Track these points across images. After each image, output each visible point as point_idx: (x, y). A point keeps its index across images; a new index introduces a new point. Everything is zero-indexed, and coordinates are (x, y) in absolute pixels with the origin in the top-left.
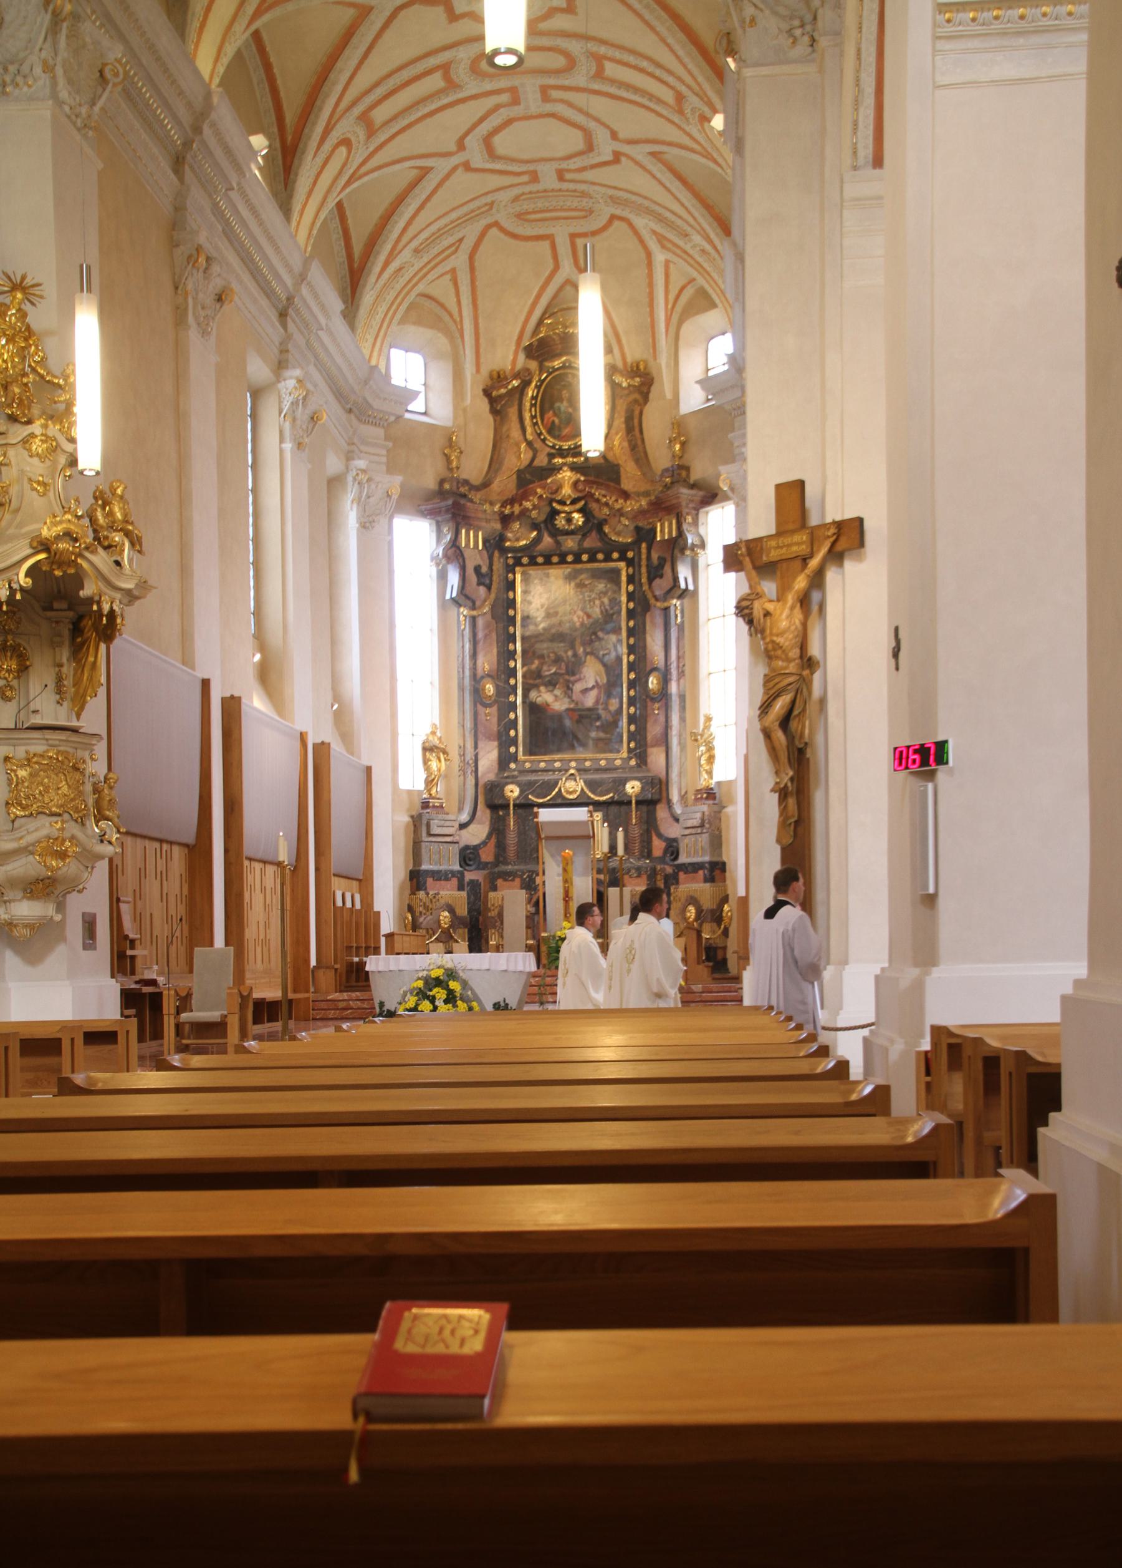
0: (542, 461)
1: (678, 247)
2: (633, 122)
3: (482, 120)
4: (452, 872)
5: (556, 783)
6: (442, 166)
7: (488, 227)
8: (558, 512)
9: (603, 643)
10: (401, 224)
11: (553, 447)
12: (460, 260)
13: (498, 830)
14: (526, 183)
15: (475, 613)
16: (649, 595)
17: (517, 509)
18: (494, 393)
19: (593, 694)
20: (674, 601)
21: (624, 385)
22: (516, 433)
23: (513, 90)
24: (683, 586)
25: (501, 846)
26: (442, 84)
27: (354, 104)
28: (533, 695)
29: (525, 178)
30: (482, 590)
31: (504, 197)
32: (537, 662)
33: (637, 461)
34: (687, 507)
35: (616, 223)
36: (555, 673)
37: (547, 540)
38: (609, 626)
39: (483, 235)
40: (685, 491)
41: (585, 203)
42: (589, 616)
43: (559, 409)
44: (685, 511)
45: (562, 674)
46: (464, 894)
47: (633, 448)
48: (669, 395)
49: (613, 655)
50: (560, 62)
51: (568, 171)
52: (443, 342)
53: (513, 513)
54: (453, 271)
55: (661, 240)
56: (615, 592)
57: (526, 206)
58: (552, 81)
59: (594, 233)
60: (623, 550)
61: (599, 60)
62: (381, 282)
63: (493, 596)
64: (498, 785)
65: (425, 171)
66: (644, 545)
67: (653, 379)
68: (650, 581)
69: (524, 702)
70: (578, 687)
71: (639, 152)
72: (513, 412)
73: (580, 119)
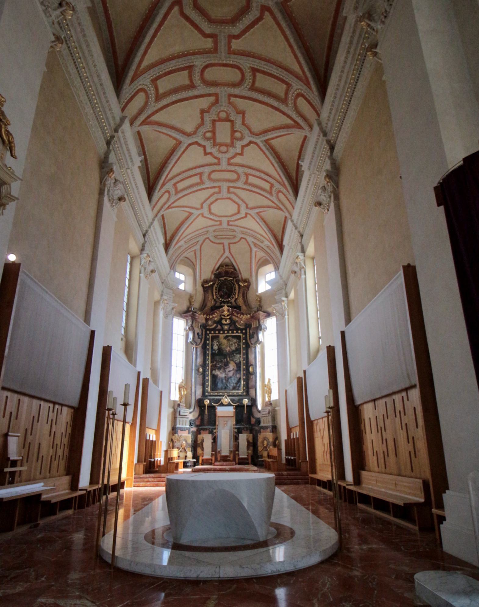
0: (218, 304)
2: (254, 200)
3: (209, 198)
5: (221, 399)
10: (182, 231)
12: (197, 247)
13: (202, 413)
14: (218, 225)
16: (250, 343)
17: (211, 317)
19: (232, 372)
22: (210, 297)
23: (219, 187)
24: (260, 340)
25: (202, 420)
26: (199, 181)
28: (214, 372)
29: (218, 223)
30: (199, 340)
33: (246, 306)
37: (219, 327)
38: (237, 352)
39: (204, 241)
40: (261, 312)
41: (234, 233)
46: (190, 435)
47: (245, 302)
48: (255, 288)
49: (238, 361)
50: (235, 176)
51: (231, 221)
52: (191, 271)
54: (195, 250)
55: (255, 245)
57: (217, 233)
59: (235, 243)
60: (241, 330)
61: (247, 175)
62: (174, 249)
65: (191, 214)
66: (248, 329)
68: (250, 339)
70: (227, 370)
73: (237, 200)
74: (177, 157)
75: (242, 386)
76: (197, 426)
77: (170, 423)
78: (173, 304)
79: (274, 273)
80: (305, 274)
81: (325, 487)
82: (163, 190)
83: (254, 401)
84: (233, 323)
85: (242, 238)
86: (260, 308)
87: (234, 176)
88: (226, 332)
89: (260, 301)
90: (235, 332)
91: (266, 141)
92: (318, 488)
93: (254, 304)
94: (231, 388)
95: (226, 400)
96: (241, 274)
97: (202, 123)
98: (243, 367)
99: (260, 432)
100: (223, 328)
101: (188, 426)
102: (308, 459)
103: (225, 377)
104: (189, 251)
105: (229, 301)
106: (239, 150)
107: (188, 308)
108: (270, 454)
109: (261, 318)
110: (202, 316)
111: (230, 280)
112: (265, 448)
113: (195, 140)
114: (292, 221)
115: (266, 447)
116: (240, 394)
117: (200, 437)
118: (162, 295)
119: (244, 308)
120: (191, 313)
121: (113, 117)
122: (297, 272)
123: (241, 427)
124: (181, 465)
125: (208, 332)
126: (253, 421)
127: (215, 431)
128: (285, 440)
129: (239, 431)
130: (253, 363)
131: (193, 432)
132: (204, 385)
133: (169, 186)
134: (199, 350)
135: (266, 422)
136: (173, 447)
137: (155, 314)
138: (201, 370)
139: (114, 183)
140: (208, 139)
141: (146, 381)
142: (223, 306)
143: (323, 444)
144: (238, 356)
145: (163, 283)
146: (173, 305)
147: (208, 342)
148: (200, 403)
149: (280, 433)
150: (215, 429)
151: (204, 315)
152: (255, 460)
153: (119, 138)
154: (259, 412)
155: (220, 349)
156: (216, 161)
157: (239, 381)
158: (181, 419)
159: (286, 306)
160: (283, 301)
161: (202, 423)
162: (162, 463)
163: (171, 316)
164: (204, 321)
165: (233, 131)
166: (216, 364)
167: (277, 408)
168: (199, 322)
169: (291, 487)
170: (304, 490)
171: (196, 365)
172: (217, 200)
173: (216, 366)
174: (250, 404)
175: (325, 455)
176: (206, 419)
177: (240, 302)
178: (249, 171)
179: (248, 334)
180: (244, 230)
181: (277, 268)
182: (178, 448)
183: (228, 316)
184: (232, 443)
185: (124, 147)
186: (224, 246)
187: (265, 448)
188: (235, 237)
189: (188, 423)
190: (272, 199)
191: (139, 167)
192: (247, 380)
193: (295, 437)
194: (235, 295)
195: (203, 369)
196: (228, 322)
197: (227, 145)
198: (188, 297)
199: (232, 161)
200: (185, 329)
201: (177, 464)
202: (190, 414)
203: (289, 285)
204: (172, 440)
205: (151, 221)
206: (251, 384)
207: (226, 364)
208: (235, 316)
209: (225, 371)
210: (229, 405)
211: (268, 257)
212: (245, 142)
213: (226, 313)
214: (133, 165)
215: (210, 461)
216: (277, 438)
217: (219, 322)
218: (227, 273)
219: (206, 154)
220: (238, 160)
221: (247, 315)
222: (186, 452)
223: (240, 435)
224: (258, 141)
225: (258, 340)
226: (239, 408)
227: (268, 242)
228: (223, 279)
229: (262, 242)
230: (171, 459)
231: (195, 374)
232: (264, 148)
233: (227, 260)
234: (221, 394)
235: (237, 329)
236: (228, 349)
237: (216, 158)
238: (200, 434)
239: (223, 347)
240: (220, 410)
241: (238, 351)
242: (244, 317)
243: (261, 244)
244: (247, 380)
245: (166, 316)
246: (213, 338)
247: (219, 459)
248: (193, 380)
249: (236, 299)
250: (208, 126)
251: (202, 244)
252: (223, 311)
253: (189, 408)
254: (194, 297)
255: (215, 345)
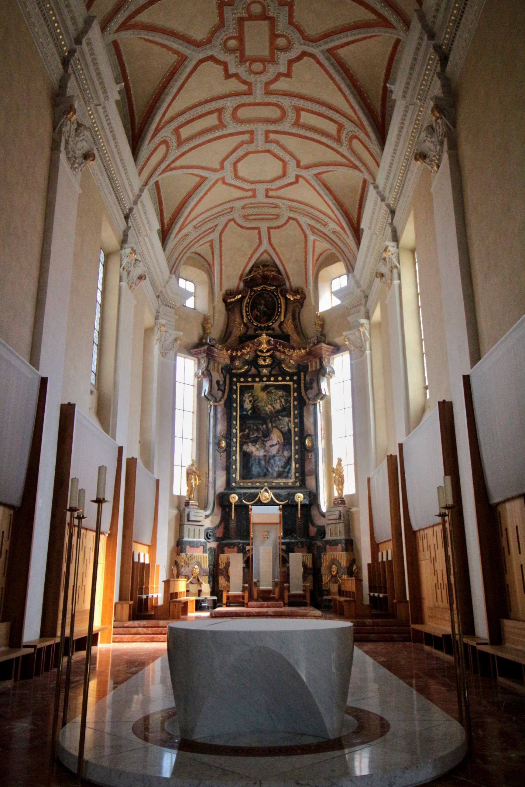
0: (251, 332)
1: (321, 232)
2: (310, 152)
4: (200, 542)
5: (257, 494)
6: (212, 177)
7: (230, 221)
8: (259, 356)
9: (281, 421)
10: (189, 209)
11: (257, 326)
12: (215, 236)
13: (225, 519)
14: (250, 197)
15: (216, 404)
16: (305, 397)
17: (239, 353)
18: (229, 301)
19: (277, 446)
20: (319, 401)
21: (292, 299)
22: (238, 320)
23: (251, 133)
24: (324, 393)
25: (227, 529)
27: (172, 119)
28: (245, 447)
29: (250, 193)
31: (238, 204)
32: (247, 430)
33: (298, 334)
34: (325, 354)
35: (291, 221)
36: (257, 436)
37: (253, 371)
38: (284, 413)
39: (226, 226)
41: (277, 211)
42: (274, 408)
43: (260, 309)
44: (324, 356)
45: (260, 437)
46: (206, 555)
47: (296, 327)
48: (313, 304)
49: (287, 428)
51: (272, 190)
52: (204, 276)
53: (237, 355)
54: (211, 241)
56: (287, 396)
57: (249, 211)
58: (272, 127)
59: (278, 227)
60: (291, 375)
63: (226, 396)
64: (225, 495)
65: (204, 179)
66: (302, 373)
67: (305, 295)
68: (306, 390)
69: (240, 451)
70: (268, 444)
71: (309, 174)
72: (237, 310)
74: (179, 83)
75: (293, 471)
76: (217, 539)
77: (173, 534)
78: (175, 332)
79: (345, 277)
80: (399, 279)
81: (438, 647)
82: (157, 140)
83: (313, 497)
84: (276, 363)
85: (290, 218)
86: (322, 337)
87: (276, 113)
88: (265, 379)
89: (322, 326)
90: (280, 378)
91: (329, 51)
92: (427, 648)
93: (311, 330)
94: (275, 474)
95: (266, 495)
96: (289, 279)
97: (221, 24)
98: (294, 438)
99: (325, 551)
100: (259, 372)
101: (202, 540)
102: (408, 599)
103: (265, 456)
104: (201, 242)
105: (269, 326)
106: (283, 69)
107: (201, 339)
108: (343, 588)
109: (325, 354)
110: (224, 351)
111: (270, 291)
112: (334, 579)
113: (209, 53)
114: (376, 187)
115: (335, 576)
116: (290, 484)
117: (223, 557)
118: (157, 318)
119: (294, 337)
120: (206, 347)
121: (73, 19)
122: (386, 275)
123: (293, 541)
124: (191, 606)
125: (235, 380)
126: (313, 530)
127: (248, 548)
128: (369, 565)
129: (290, 549)
130: (312, 433)
131: (211, 548)
132: (228, 469)
133: (167, 133)
134: (219, 409)
135: (334, 533)
136: (178, 576)
137: (146, 350)
138: (223, 444)
139: (76, 130)
140: (231, 51)
141: (132, 462)
142: (261, 335)
143: (435, 573)
144: (287, 419)
145: (158, 297)
146: (175, 334)
147: (234, 396)
148: (222, 501)
149: (358, 552)
150: (248, 544)
151: (227, 351)
152: (317, 598)
153: (82, 53)
154: (323, 515)
155: (255, 408)
156: (245, 88)
157: (288, 462)
158: (192, 528)
159: (367, 334)
160: (362, 325)
161: (226, 534)
162: (160, 602)
163: (172, 353)
164: (228, 361)
165: (274, 36)
166: (248, 434)
167: (354, 510)
168: (219, 363)
169: (381, 647)
170: (403, 652)
171: (215, 436)
172: (247, 154)
173: (248, 438)
174: (307, 502)
175: (439, 591)
176: (234, 529)
177: (289, 327)
178: (301, 103)
179: (302, 382)
180: (295, 204)
181: (350, 269)
182: (187, 577)
183: (267, 351)
184: (278, 569)
185: (92, 68)
186: (259, 233)
187: (334, 579)
188: (278, 216)
189: (203, 535)
190: (340, 150)
191: (117, 102)
192: (302, 462)
193: (385, 559)
194: (279, 316)
195: (227, 442)
196: (268, 361)
197: (262, 60)
198: (200, 320)
199: (273, 87)
200: (196, 375)
201: (186, 603)
202: (206, 520)
203: (371, 298)
204: (176, 563)
205: (137, 191)
206: (309, 467)
207: (267, 435)
208: (279, 351)
209: (263, 446)
210: (271, 503)
211: (334, 251)
212: (293, 54)
213: (264, 346)
214: (107, 98)
215: (241, 600)
216: (354, 561)
217: (254, 362)
218: (265, 279)
219: (228, 76)
220: (282, 85)
221: (300, 349)
222: (200, 584)
223: (291, 554)
224: (315, 51)
225: (319, 394)
226: (289, 509)
227: (335, 224)
228: (259, 288)
229: (325, 225)
230: (175, 595)
231: (214, 450)
232: (326, 64)
233: (265, 257)
234: (258, 484)
235: (284, 374)
236: (268, 408)
237: (244, 82)
238: (223, 552)
239: (260, 404)
240: (257, 513)
241: (285, 411)
242: (297, 354)
243: (322, 229)
244: (302, 462)
245: (164, 353)
246: (244, 389)
247: (255, 595)
248: (211, 461)
249: (281, 323)
250: (231, 29)
251: (223, 230)
252: (260, 343)
253: (205, 508)
254: (211, 321)
255: (247, 401)
